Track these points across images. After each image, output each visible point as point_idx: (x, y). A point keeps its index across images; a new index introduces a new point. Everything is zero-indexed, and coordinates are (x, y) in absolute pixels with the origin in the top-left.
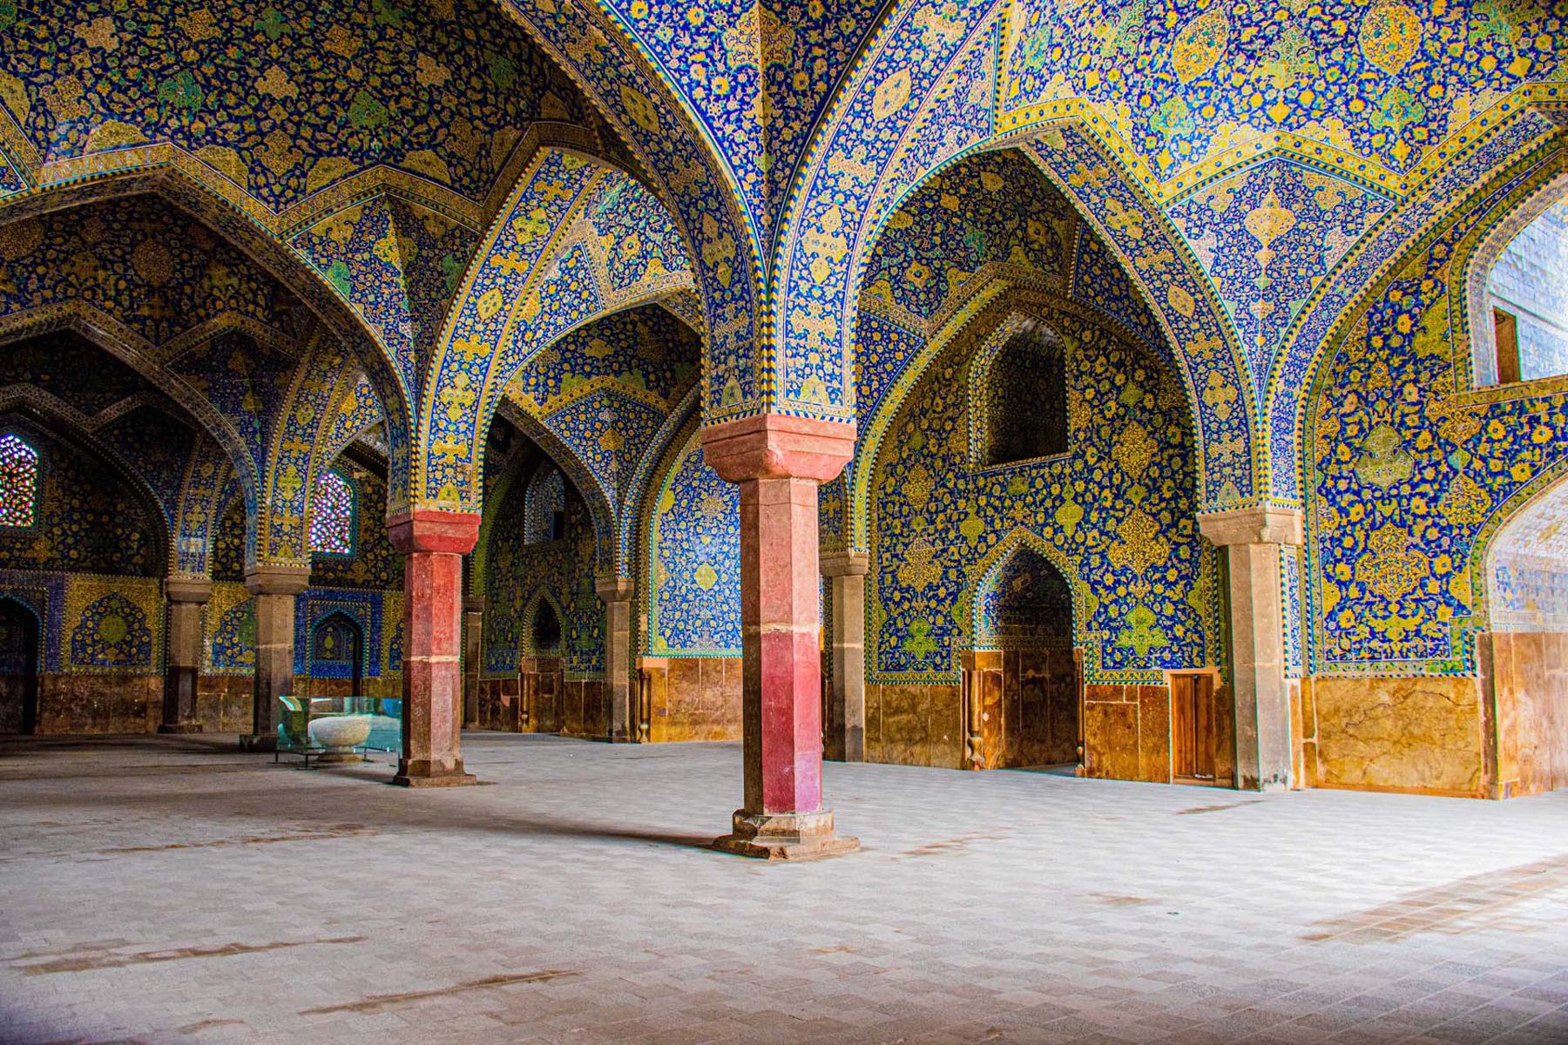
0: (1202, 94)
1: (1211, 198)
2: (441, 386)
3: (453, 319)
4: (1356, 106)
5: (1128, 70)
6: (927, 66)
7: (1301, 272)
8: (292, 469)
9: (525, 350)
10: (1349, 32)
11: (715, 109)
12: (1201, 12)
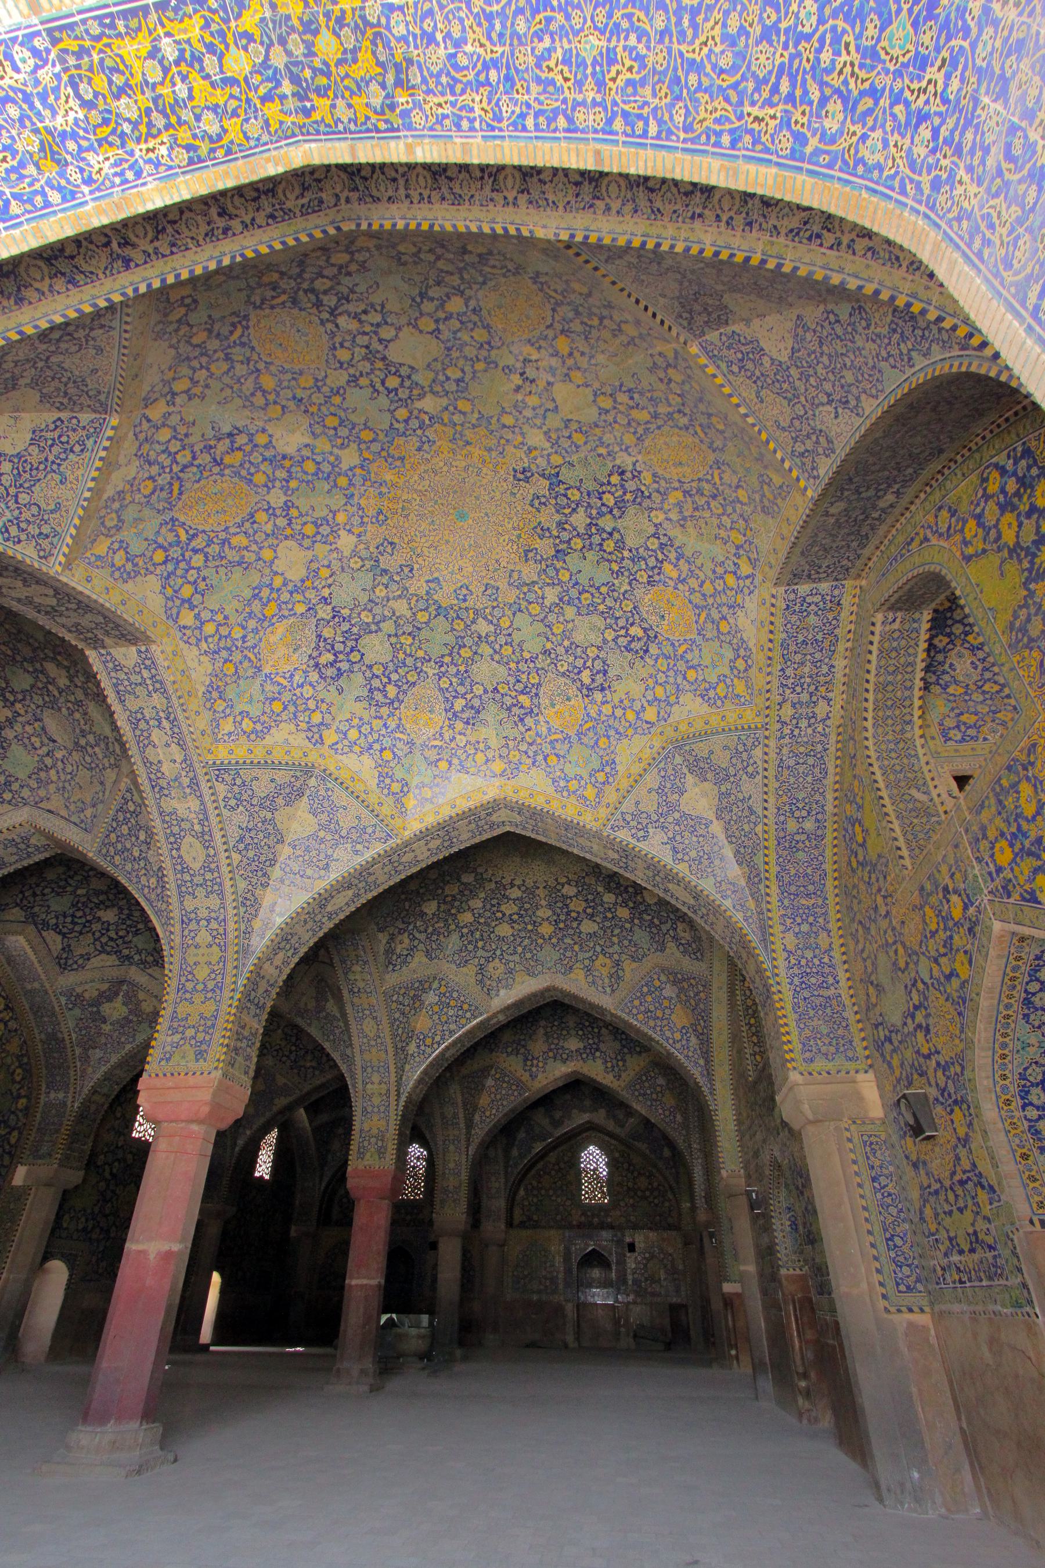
0: (591, 734)
1: (637, 803)
2: (364, 1084)
3: (355, 1040)
4: (691, 675)
5: (524, 747)
6: (197, 828)
7: (746, 827)
8: (452, 1148)
9: (428, 1050)
10: (645, 630)
11: (153, 896)
12: (539, 684)
